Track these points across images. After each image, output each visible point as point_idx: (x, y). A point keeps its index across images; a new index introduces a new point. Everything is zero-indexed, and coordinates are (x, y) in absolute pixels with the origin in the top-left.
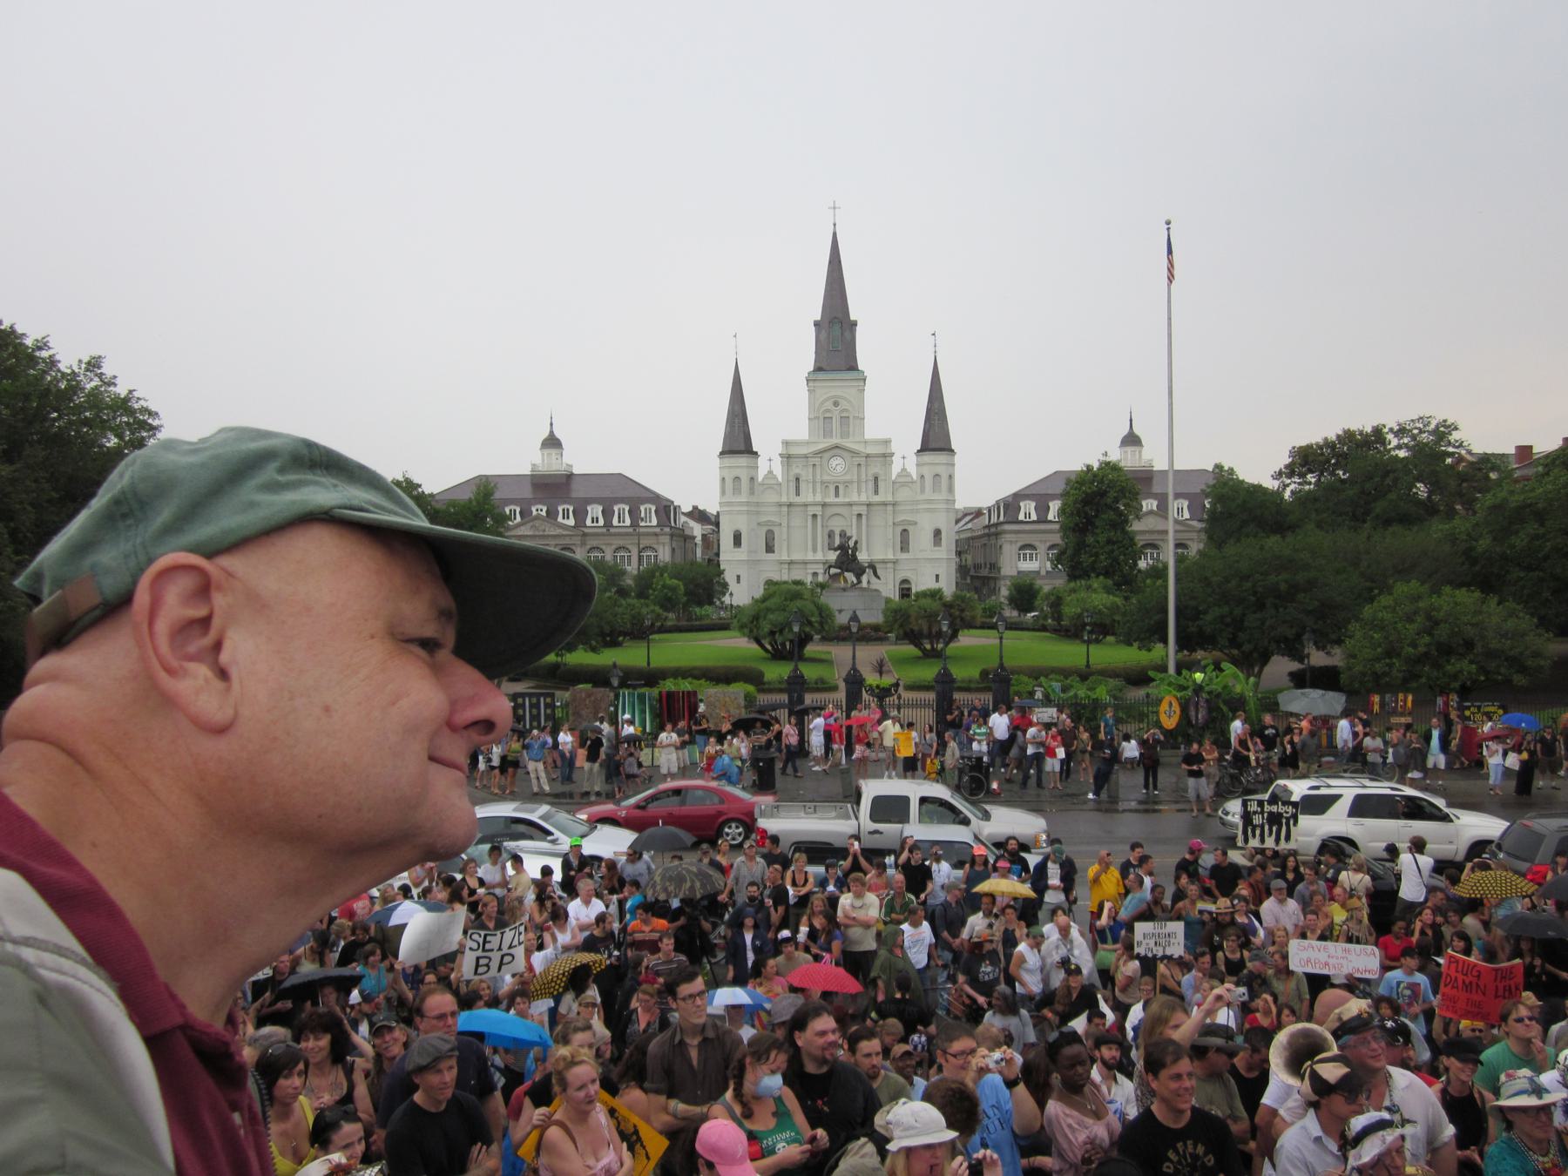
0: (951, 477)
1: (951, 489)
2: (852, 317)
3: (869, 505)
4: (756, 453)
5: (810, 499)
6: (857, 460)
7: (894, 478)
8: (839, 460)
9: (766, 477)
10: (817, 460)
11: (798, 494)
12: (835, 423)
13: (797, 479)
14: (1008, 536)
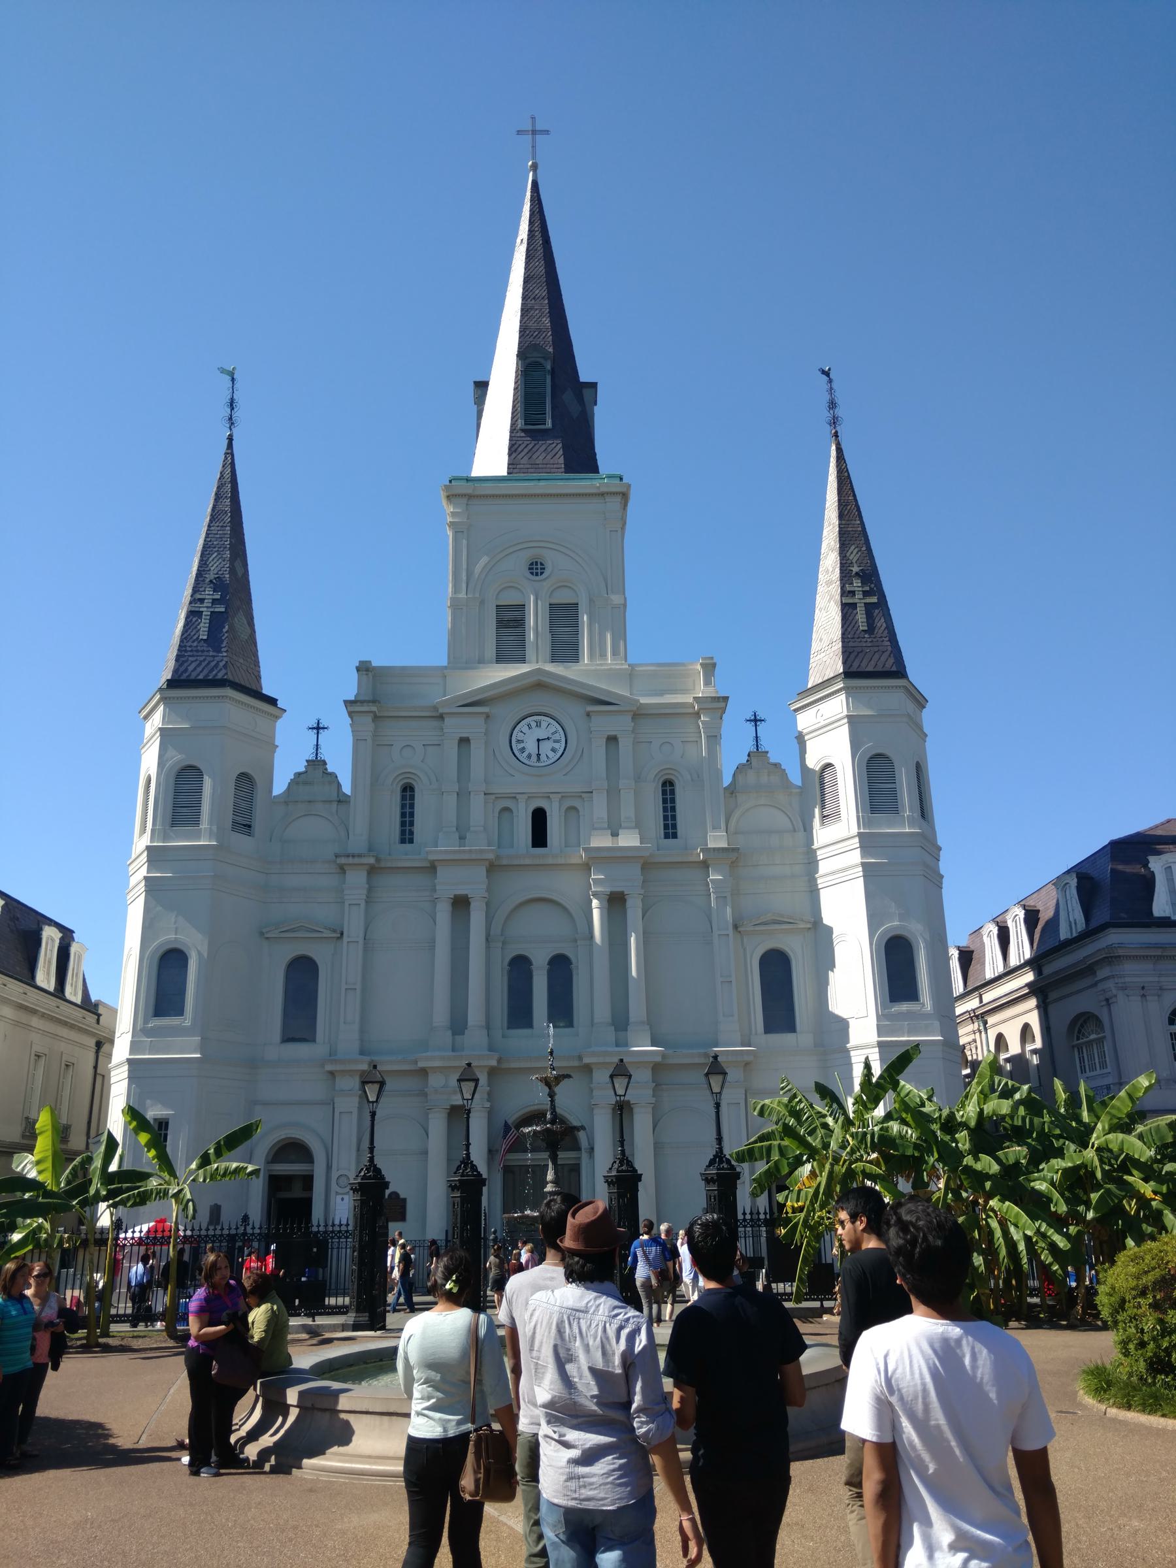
0: (920, 772)
1: (924, 811)
2: (584, 376)
3: (648, 865)
4: (273, 702)
5: (446, 847)
6: (605, 724)
7: (727, 780)
8: (547, 728)
9: (299, 779)
10: (472, 726)
11: (407, 836)
12: (535, 621)
13: (408, 791)
14: (1128, 967)
